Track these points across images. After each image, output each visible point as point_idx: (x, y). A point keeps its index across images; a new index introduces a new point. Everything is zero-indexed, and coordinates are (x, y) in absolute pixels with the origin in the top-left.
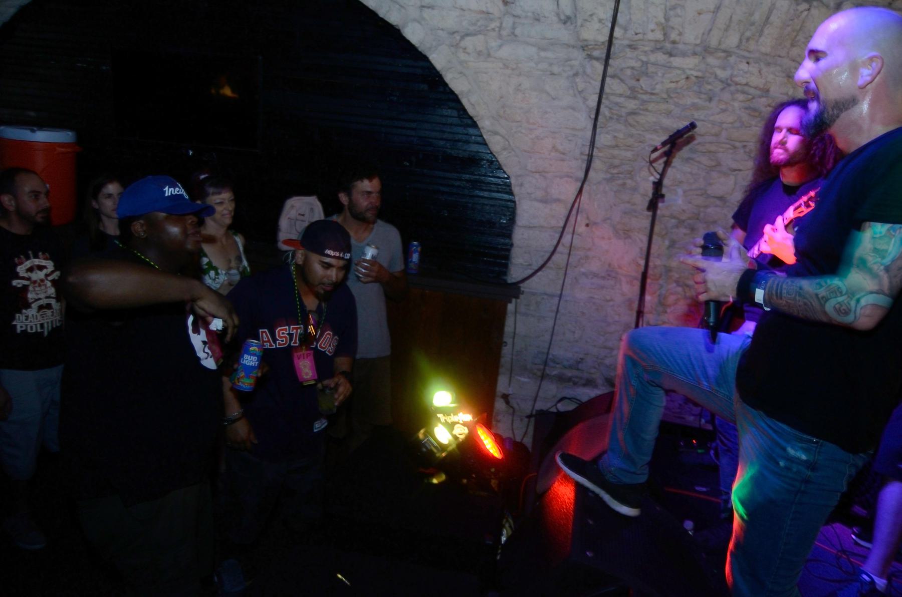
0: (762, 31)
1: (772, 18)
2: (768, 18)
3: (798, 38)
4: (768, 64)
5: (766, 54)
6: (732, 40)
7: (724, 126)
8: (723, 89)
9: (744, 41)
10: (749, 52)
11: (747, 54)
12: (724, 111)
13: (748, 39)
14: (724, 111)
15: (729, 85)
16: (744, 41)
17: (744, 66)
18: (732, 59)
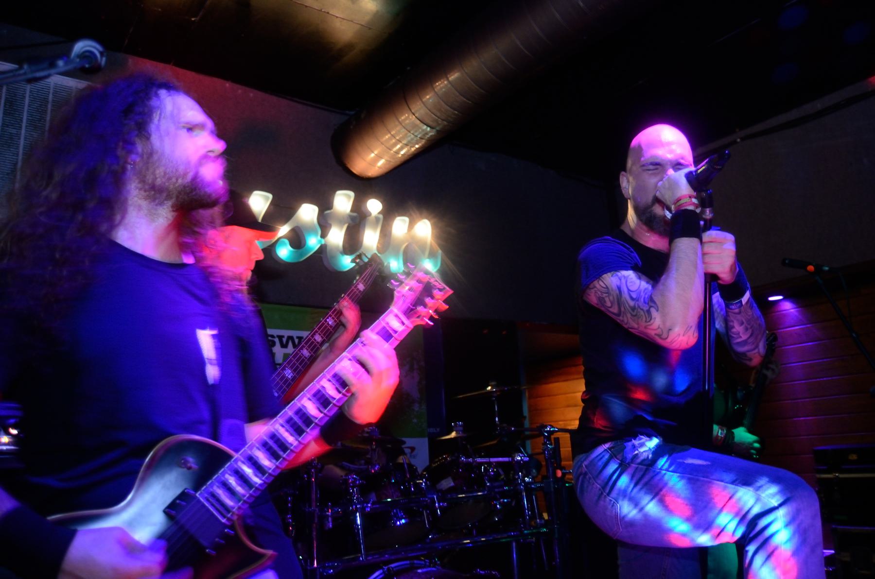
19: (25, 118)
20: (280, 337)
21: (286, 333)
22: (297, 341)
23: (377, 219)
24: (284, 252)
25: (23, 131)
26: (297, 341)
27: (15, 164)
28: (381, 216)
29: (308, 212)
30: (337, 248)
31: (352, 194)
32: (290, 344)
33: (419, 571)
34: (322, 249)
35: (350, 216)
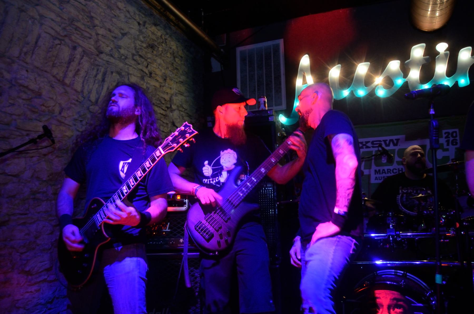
0: (34, 50)
1: (40, 43)
2: (36, 42)
3: (55, 62)
4: (39, 75)
5: (37, 68)
6: (15, 52)
7: (14, 117)
8: (10, 88)
9: (23, 54)
10: (27, 63)
11: (25, 65)
12: (13, 105)
13: (26, 54)
14: (13, 105)
15: (15, 85)
16: (23, 54)
17: (24, 72)
18: (15, 66)
19: (256, 66)
20: (385, 141)
21: (388, 138)
22: (395, 142)
23: (446, 55)
24: (381, 93)
25: (256, 72)
26: (395, 142)
27: (255, 87)
28: (448, 52)
29: (394, 65)
30: (417, 81)
31: (424, 44)
32: (391, 144)
33: (383, 276)
34: (406, 85)
35: (425, 59)
